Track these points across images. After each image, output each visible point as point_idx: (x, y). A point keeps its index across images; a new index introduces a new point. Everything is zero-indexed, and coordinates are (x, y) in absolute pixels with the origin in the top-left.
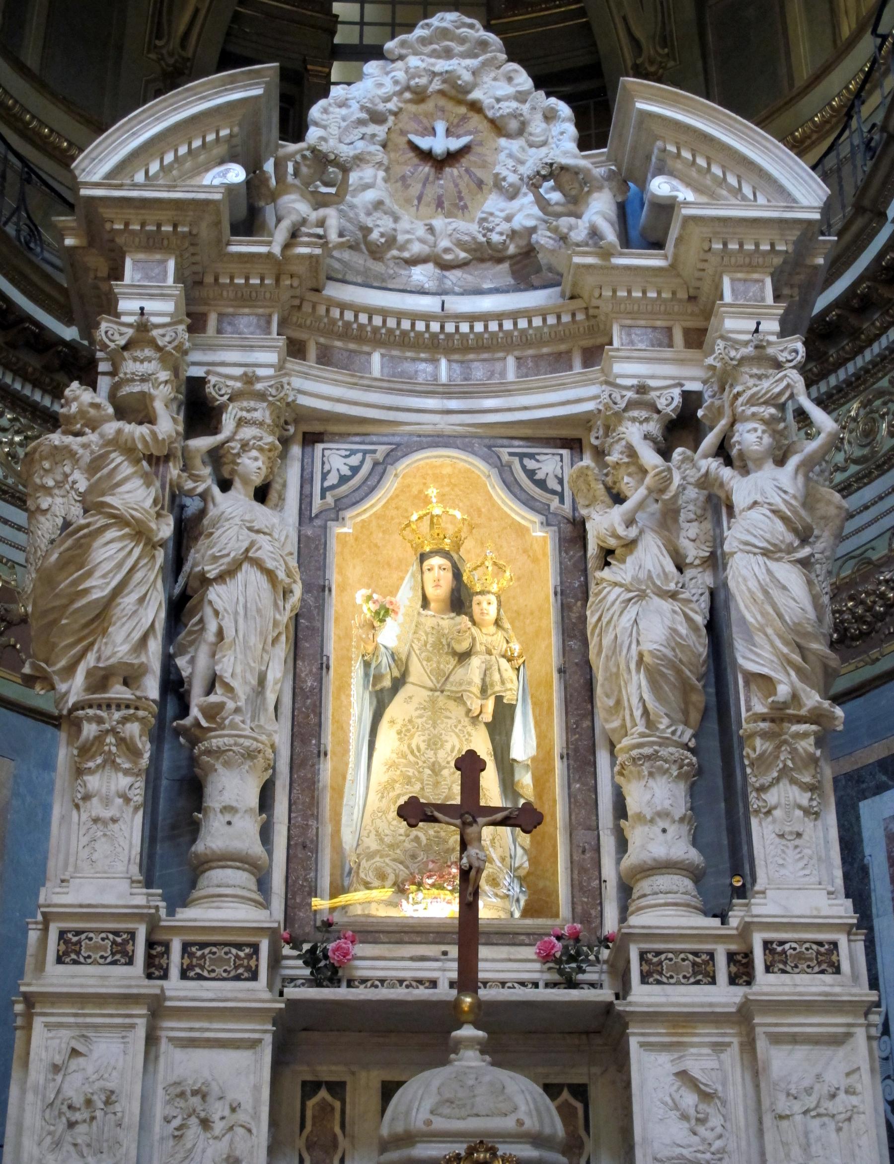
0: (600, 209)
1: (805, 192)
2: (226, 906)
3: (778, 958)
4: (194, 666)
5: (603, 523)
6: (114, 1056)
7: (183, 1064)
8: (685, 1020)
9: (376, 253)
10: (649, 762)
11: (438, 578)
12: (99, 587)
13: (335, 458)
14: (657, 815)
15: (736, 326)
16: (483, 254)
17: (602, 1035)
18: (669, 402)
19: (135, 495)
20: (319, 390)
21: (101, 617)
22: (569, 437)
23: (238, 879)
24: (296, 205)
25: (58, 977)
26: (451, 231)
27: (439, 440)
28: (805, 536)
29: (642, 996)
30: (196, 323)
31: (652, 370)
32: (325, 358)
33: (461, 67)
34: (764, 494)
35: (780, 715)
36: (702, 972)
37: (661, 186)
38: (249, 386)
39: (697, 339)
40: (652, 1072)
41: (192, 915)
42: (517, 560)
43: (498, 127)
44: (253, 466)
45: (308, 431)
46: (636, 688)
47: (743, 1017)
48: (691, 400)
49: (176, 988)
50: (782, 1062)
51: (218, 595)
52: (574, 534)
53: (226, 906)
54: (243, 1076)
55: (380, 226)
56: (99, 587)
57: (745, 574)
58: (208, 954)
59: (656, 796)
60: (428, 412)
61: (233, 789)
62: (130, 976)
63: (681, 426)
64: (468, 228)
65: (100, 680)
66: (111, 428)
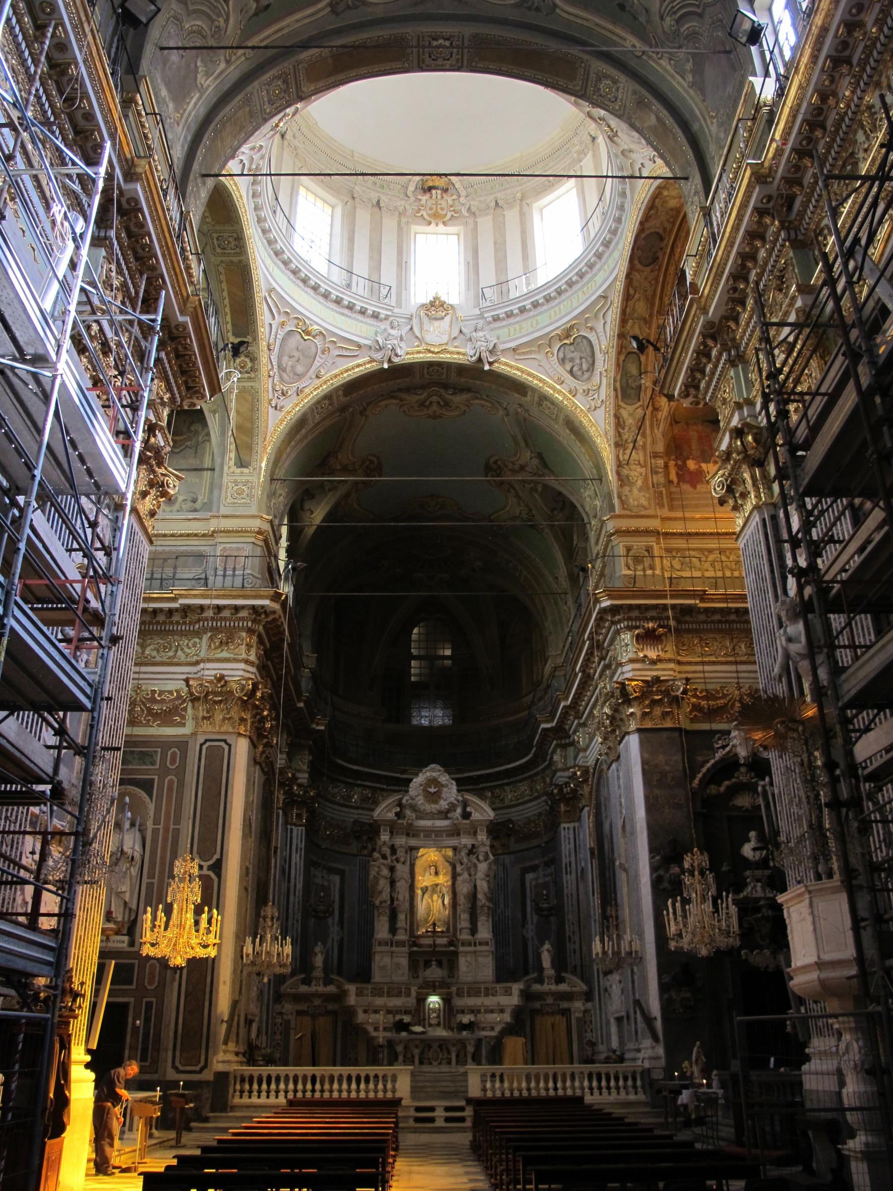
0: (459, 810)
1: (491, 814)
2: (401, 936)
3: (480, 944)
4: (395, 896)
5: (459, 869)
6: (387, 960)
7: (395, 960)
8: (467, 953)
9: (421, 815)
10: (464, 911)
11: (433, 870)
12: (380, 888)
14: (464, 921)
15: (480, 838)
16: (440, 812)
17: (456, 954)
18: (470, 847)
19: (385, 872)
20: (413, 842)
21: (380, 892)
23: (403, 931)
24: (408, 812)
25: (378, 949)
26: (434, 807)
28: (488, 876)
29: (461, 949)
30: (392, 833)
31: (466, 841)
32: (414, 836)
34: (483, 867)
35: (482, 907)
36: (470, 945)
37: (468, 809)
38: (401, 846)
39: (475, 833)
40: (462, 960)
41: (396, 938)
43: (443, 786)
44: (402, 859)
46: (462, 898)
47: (475, 952)
48: (473, 846)
49: (394, 949)
50: (480, 959)
51: (398, 884)
52: (454, 867)
53: (401, 936)
54: (404, 962)
55: (422, 808)
56: (380, 888)
57: (479, 883)
59: (465, 916)
61: (401, 917)
62: (388, 948)
63: (472, 851)
64: (437, 807)
65: (381, 903)
66: (382, 861)
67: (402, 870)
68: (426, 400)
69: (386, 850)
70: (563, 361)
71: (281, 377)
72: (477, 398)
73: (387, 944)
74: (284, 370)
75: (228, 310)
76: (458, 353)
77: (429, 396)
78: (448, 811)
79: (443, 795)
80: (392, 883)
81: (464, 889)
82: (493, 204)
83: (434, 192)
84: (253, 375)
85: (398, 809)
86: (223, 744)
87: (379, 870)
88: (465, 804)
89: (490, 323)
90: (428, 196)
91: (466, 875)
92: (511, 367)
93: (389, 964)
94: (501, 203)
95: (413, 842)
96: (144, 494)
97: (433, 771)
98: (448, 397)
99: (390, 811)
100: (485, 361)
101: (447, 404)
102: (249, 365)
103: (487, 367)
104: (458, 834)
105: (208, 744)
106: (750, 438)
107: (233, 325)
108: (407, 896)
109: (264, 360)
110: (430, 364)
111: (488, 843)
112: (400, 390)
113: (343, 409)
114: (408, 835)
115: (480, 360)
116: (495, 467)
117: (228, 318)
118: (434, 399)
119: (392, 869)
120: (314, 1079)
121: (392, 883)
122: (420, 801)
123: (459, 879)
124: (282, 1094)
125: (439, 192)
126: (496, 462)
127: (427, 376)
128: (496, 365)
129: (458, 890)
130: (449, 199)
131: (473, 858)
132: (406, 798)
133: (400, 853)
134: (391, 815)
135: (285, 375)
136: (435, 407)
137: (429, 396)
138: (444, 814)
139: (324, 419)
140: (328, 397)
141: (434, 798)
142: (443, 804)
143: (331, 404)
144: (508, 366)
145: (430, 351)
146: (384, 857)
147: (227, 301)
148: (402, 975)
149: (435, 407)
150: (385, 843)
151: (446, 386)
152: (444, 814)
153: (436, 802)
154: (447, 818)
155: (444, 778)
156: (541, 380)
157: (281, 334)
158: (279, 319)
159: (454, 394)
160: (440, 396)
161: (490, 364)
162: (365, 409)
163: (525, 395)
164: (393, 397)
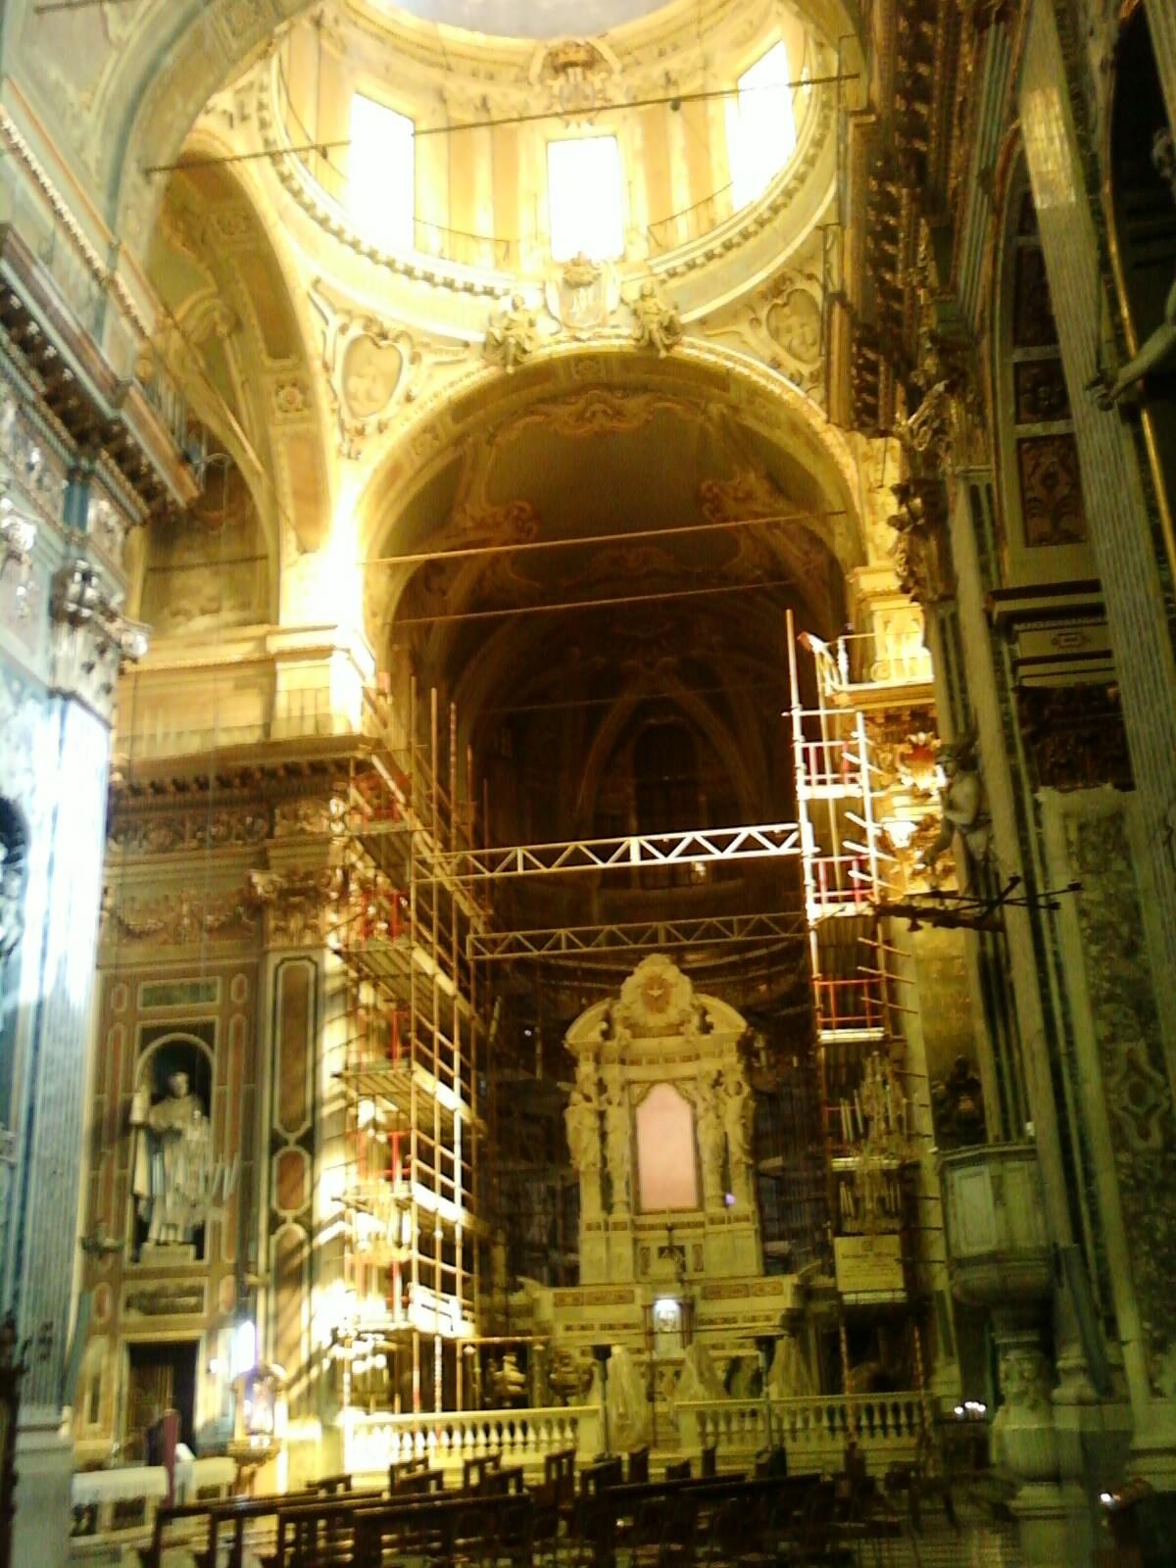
0: (696, 1020)
2: (621, 1214)
3: (738, 1220)
12: (584, 1144)
13: (637, 1090)
16: (670, 1026)
18: (714, 1075)
19: (591, 1121)
22: (693, 1079)
27: (661, 1082)
31: (710, 1066)
33: (657, 969)
36: (722, 1222)
42: (682, 1115)
44: (615, 1100)
45: (630, 1083)
48: (720, 1074)
55: (642, 1020)
58: (617, 1226)
60: (657, 1072)
63: (717, 1083)
67: (616, 1117)
68: (585, 410)
69: (592, 1091)
70: (775, 334)
71: (351, 409)
72: (660, 399)
73: (599, 1227)
74: (355, 398)
75: (254, 321)
76: (618, 337)
77: (590, 403)
78: (682, 1024)
79: (673, 999)
80: (603, 1136)
81: (709, 1139)
82: (662, 81)
83: (570, 71)
84: (306, 412)
85: (604, 1026)
86: (306, 963)
87: (579, 1120)
88: (704, 1013)
89: (663, 282)
90: (562, 79)
91: (711, 1116)
92: (700, 349)
93: (599, 1252)
94: (673, 77)
95: (634, 1073)
96: (89, 668)
97: (656, 966)
98: (617, 402)
99: (591, 1029)
100: (659, 344)
101: (619, 413)
102: (299, 397)
103: (663, 354)
104: (698, 1057)
105: (287, 964)
106: (918, 501)
107: (267, 341)
108: (627, 1152)
109: (321, 387)
110: (579, 359)
111: (740, 1067)
112: (542, 401)
113: (458, 441)
114: (623, 1062)
115: (651, 343)
116: (709, 495)
117: (258, 333)
118: (601, 406)
119: (602, 1116)
120: (574, 1423)
121: (603, 1136)
122: (640, 1012)
123: (702, 1124)
124: (457, 1449)
125: (579, 70)
126: (710, 489)
127: (577, 377)
128: (677, 349)
129: (701, 1138)
130: (596, 79)
131: (720, 1090)
132: (617, 1006)
133: (614, 1092)
134: (595, 1036)
135: (356, 406)
136: (601, 420)
137: (590, 403)
138: (675, 1029)
139: (432, 459)
140: (429, 429)
141: (658, 1004)
142: (672, 1015)
143: (436, 438)
144: (695, 349)
145: (578, 339)
146: (588, 1099)
147: (251, 309)
148: (624, 1272)
149: (601, 420)
150: (588, 1077)
151: (609, 387)
152: (675, 1029)
153: (661, 1010)
154: (679, 1034)
155: (672, 973)
156: (746, 365)
157: (343, 343)
158: (336, 321)
159: (624, 397)
160: (605, 402)
161: (668, 348)
162: (493, 436)
163: (725, 388)
164: (532, 413)
